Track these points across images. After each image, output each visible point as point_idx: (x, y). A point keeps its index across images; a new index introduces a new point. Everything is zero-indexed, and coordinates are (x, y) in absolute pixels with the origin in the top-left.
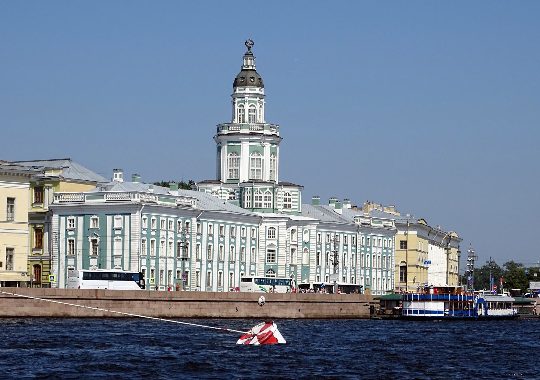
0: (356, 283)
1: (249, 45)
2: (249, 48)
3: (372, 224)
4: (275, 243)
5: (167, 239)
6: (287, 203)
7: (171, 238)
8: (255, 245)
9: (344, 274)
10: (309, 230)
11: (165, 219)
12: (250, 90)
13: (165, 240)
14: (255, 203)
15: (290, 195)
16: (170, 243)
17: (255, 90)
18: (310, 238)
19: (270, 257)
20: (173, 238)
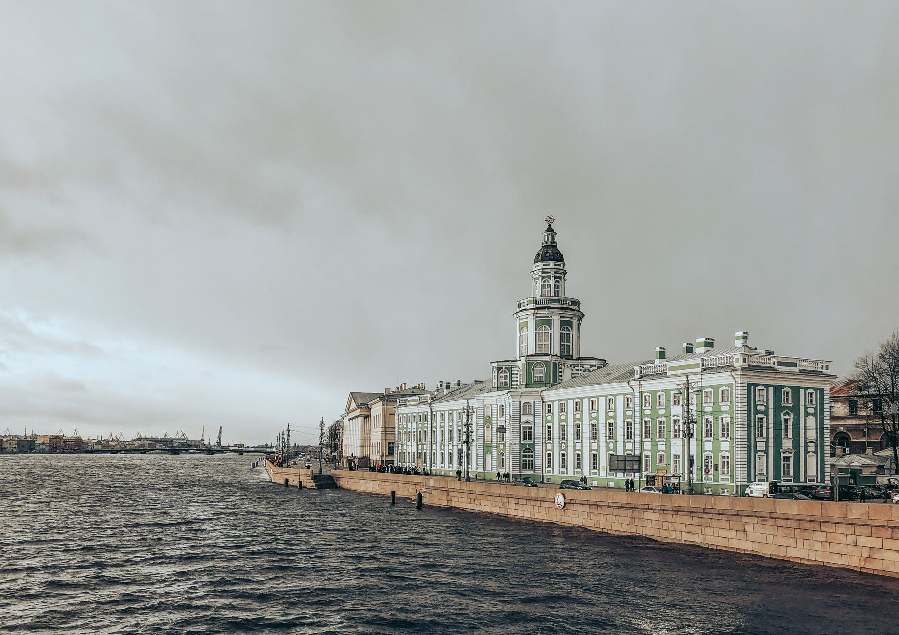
7: (414, 428)
9: (611, 450)
11: (411, 415)
13: (410, 430)
16: (414, 432)
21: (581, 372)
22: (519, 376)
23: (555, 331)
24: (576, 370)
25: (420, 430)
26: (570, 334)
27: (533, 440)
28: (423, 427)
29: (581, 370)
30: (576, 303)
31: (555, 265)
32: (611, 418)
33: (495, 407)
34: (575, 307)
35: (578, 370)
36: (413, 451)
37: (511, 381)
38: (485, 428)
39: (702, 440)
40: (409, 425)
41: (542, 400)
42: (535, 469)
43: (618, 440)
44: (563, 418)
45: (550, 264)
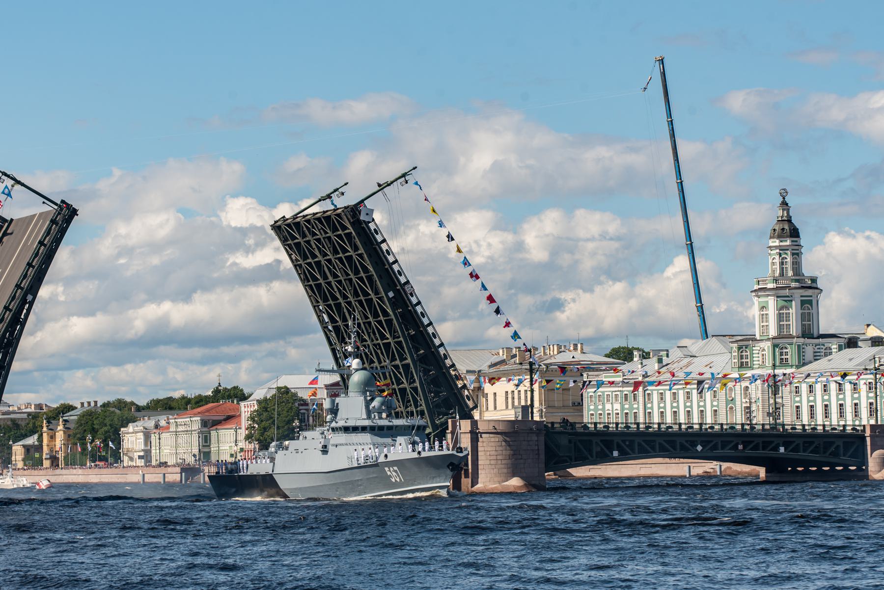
1: (784, 193)
2: (784, 198)
5: (612, 411)
7: (616, 410)
8: (717, 406)
12: (773, 242)
16: (618, 414)
20: (619, 409)
21: (822, 350)
22: (760, 355)
24: (818, 349)
25: (626, 411)
28: (631, 408)
29: (822, 348)
30: (814, 280)
31: (792, 241)
32: (856, 399)
34: (814, 285)
35: (819, 349)
38: (728, 409)
40: (608, 406)
43: (862, 417)
44: (811, 398)
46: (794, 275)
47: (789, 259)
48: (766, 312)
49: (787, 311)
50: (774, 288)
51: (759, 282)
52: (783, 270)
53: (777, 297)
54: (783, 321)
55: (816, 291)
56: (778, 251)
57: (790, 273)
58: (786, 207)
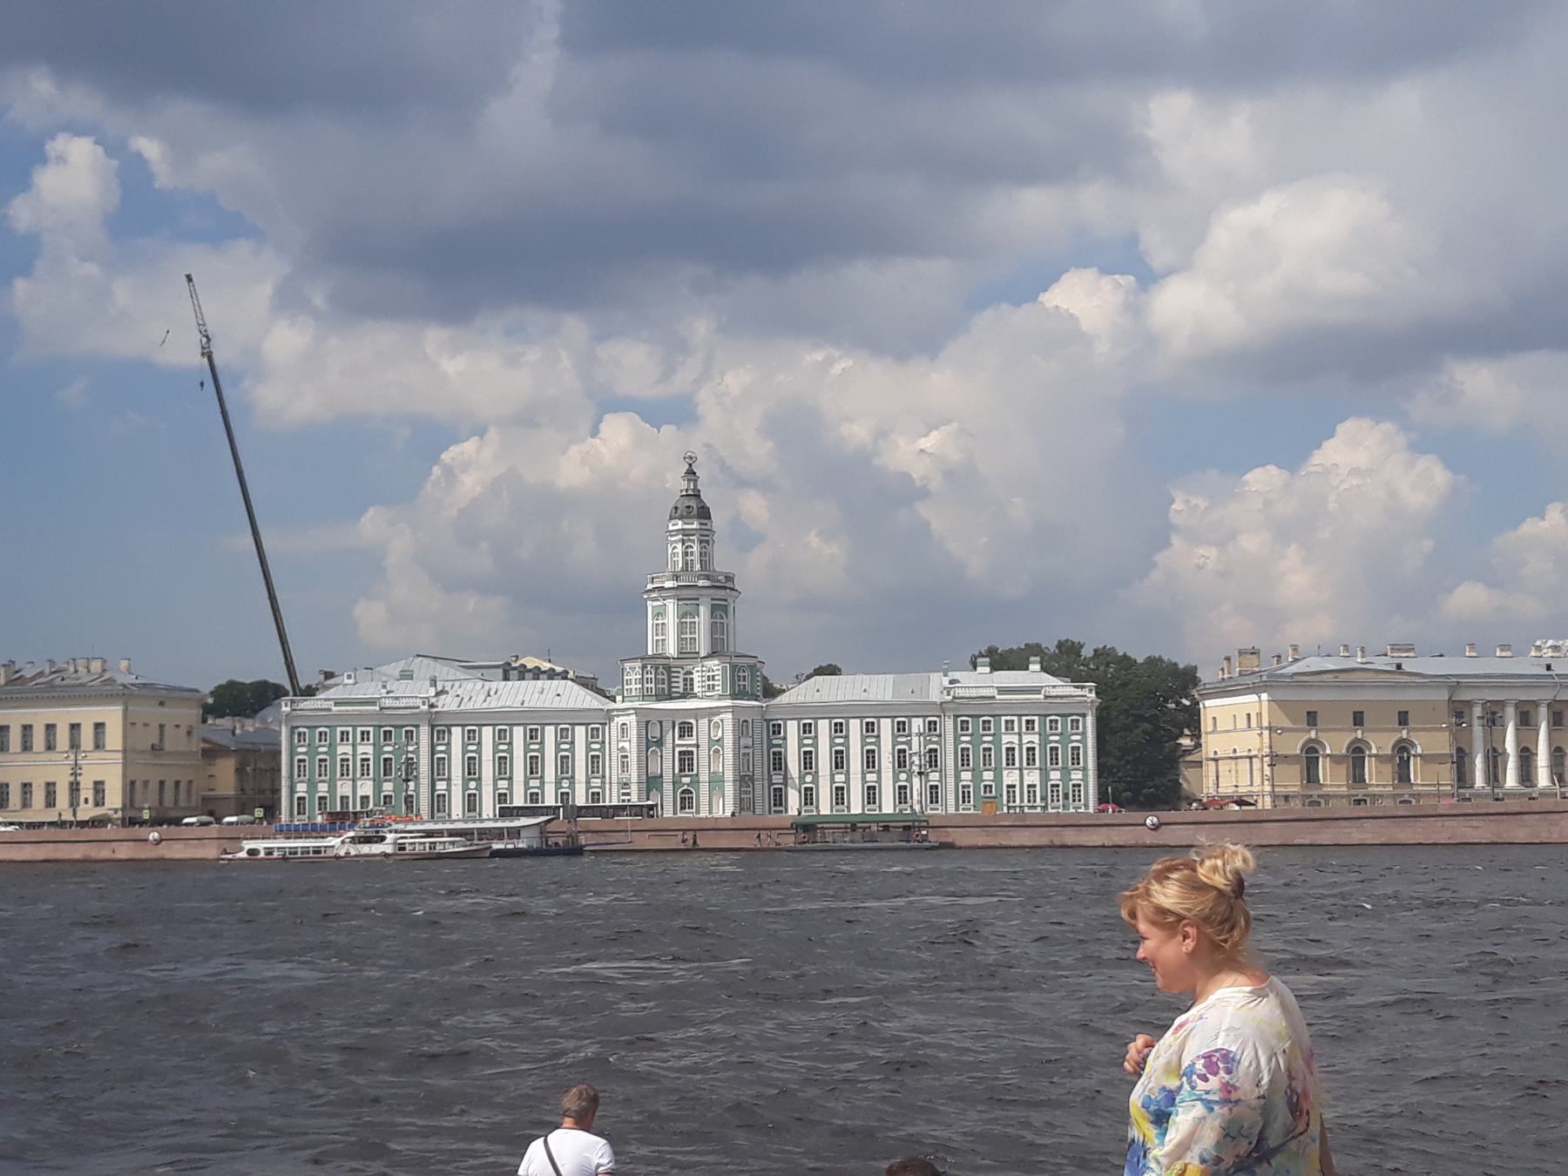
0: (611, 802)
1: (691, 460)
2: (690, 465)
3: (998, 697)
4: (626, 745)
5: (354, 755)
6: (711, 683)
8: (602, 749)
10: (722, 721)
11: (350, 729)
12: (673, 525)
13: (351, 758)
14: (627, 690)
15: (713, 671)
17: (677, 524)
18: (723, 733)
19: (689, 765)
20: (371, 752)
22: (681, 680)
23: (703, 618)
26: (695, 623)
27: (751, 770)
30: (729, 578)
33: (667, 725)
36: (360, 793)
37: (670, 687)
38: (649, 753)
39: (1046, 769)
40: (343, 749)
41: (762, 717)
42: (754, 809)
45: (706, 524)
46: (702, 570)
47: (696, 549)
48: (663, 621)
49: (722, 621)
50: (674, 588)
51: (653, 578)
52: (687, 564)
53: (679, 600)
54: (687, 634)
55: (734, 593)
56: (680, 537)
57: (698, 567)
58: (693, 477)
